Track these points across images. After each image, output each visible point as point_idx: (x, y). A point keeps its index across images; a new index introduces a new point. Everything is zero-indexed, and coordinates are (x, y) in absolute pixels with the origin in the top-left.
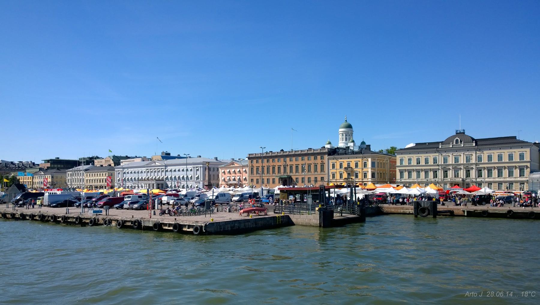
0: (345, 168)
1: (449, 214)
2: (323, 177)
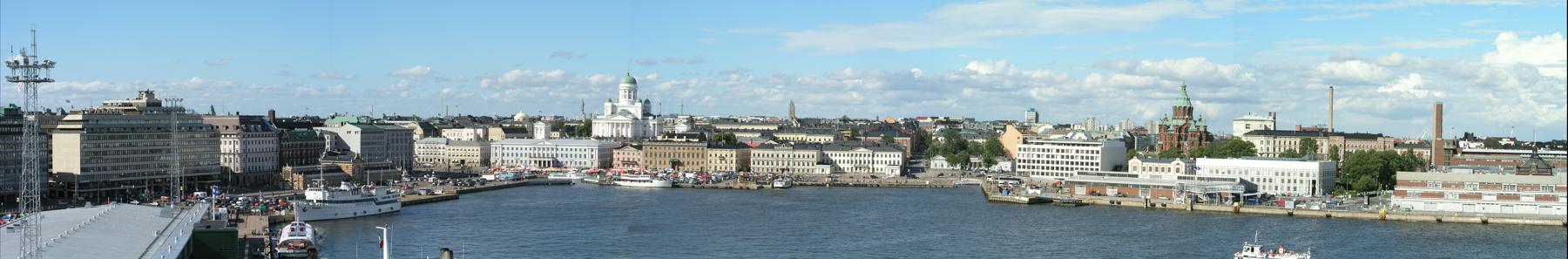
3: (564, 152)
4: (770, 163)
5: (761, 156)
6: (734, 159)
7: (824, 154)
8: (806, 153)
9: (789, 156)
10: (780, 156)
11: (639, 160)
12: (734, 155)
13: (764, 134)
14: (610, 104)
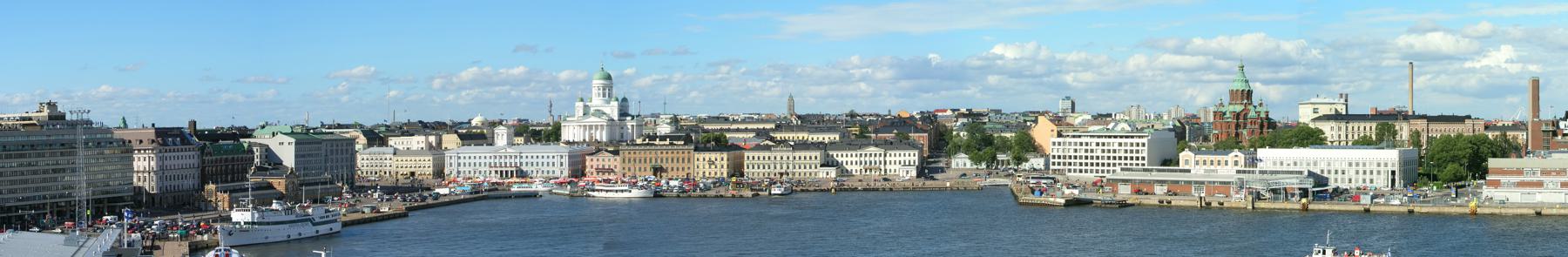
3: (530, 160)
4: (767, 167)
5: (756, 158)
6: (725, 163)
7: (828, 155)
8: (808, 154)
9: (788, 158)
10: (779, 158)
11: (616, 167)
12: (725, 159)
13: (760, 133)
14: (581, 104)
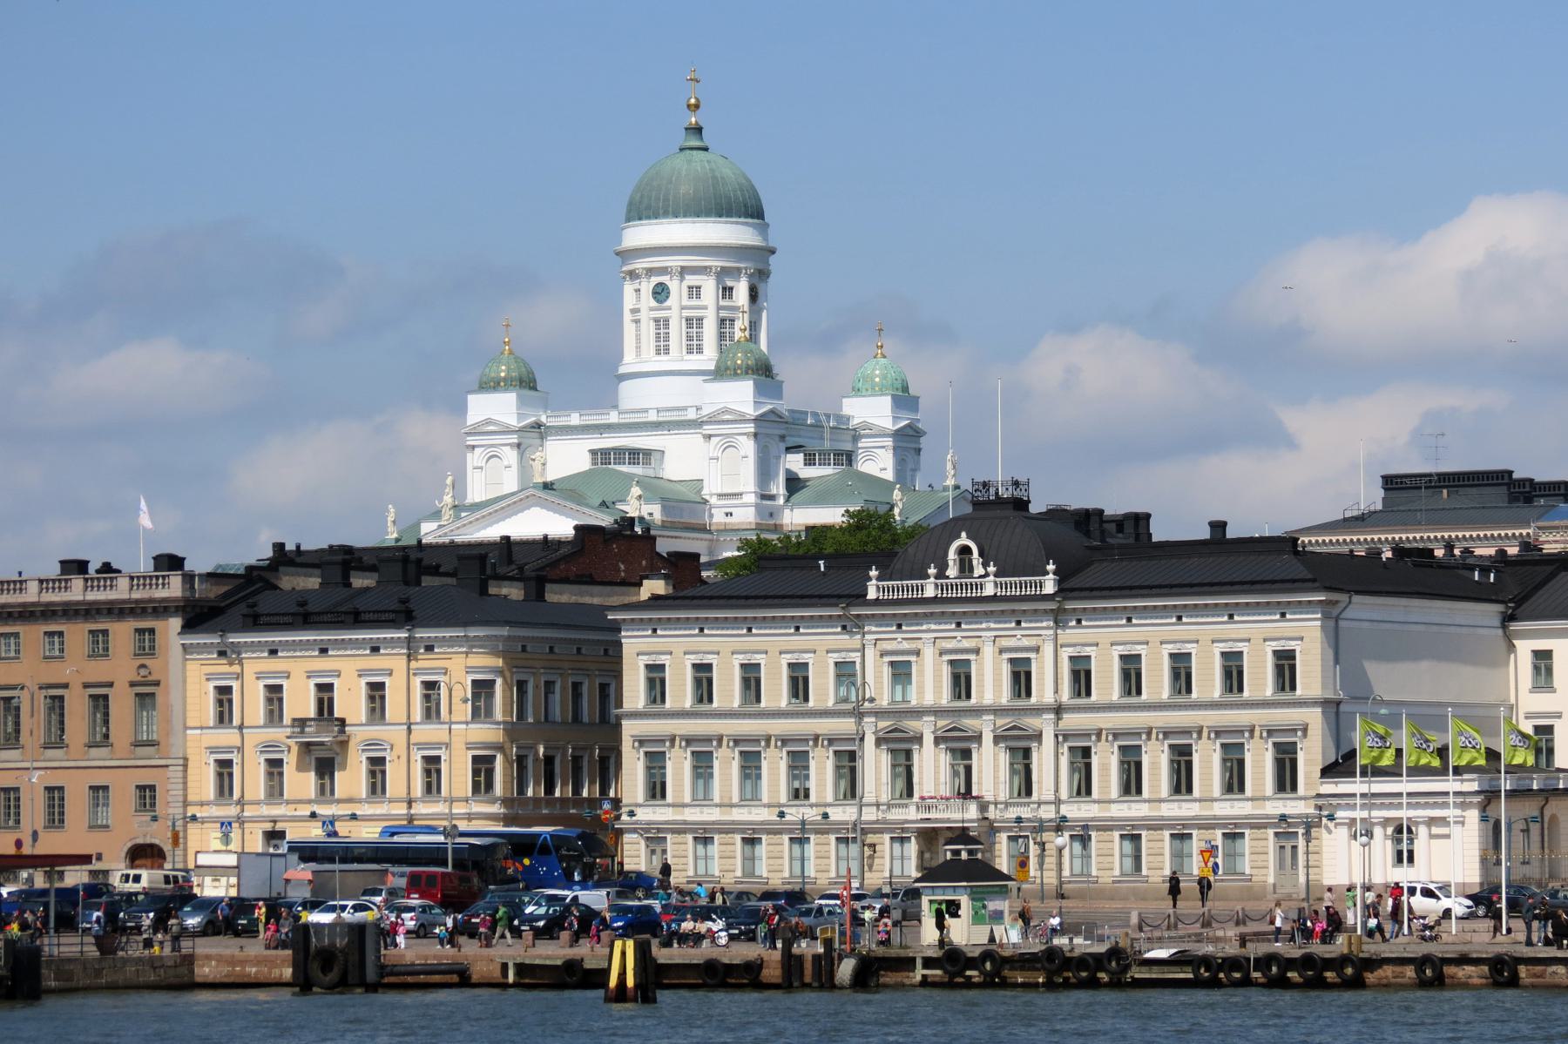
0: (301, 723)
1: (455, 978)
2: (152, 788)
9: (1022, 680)
